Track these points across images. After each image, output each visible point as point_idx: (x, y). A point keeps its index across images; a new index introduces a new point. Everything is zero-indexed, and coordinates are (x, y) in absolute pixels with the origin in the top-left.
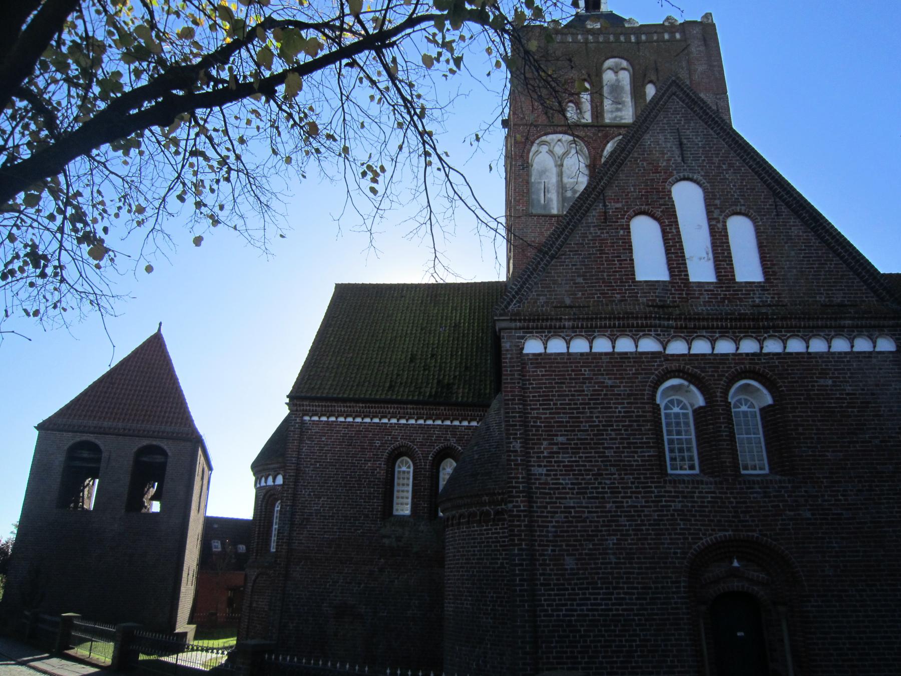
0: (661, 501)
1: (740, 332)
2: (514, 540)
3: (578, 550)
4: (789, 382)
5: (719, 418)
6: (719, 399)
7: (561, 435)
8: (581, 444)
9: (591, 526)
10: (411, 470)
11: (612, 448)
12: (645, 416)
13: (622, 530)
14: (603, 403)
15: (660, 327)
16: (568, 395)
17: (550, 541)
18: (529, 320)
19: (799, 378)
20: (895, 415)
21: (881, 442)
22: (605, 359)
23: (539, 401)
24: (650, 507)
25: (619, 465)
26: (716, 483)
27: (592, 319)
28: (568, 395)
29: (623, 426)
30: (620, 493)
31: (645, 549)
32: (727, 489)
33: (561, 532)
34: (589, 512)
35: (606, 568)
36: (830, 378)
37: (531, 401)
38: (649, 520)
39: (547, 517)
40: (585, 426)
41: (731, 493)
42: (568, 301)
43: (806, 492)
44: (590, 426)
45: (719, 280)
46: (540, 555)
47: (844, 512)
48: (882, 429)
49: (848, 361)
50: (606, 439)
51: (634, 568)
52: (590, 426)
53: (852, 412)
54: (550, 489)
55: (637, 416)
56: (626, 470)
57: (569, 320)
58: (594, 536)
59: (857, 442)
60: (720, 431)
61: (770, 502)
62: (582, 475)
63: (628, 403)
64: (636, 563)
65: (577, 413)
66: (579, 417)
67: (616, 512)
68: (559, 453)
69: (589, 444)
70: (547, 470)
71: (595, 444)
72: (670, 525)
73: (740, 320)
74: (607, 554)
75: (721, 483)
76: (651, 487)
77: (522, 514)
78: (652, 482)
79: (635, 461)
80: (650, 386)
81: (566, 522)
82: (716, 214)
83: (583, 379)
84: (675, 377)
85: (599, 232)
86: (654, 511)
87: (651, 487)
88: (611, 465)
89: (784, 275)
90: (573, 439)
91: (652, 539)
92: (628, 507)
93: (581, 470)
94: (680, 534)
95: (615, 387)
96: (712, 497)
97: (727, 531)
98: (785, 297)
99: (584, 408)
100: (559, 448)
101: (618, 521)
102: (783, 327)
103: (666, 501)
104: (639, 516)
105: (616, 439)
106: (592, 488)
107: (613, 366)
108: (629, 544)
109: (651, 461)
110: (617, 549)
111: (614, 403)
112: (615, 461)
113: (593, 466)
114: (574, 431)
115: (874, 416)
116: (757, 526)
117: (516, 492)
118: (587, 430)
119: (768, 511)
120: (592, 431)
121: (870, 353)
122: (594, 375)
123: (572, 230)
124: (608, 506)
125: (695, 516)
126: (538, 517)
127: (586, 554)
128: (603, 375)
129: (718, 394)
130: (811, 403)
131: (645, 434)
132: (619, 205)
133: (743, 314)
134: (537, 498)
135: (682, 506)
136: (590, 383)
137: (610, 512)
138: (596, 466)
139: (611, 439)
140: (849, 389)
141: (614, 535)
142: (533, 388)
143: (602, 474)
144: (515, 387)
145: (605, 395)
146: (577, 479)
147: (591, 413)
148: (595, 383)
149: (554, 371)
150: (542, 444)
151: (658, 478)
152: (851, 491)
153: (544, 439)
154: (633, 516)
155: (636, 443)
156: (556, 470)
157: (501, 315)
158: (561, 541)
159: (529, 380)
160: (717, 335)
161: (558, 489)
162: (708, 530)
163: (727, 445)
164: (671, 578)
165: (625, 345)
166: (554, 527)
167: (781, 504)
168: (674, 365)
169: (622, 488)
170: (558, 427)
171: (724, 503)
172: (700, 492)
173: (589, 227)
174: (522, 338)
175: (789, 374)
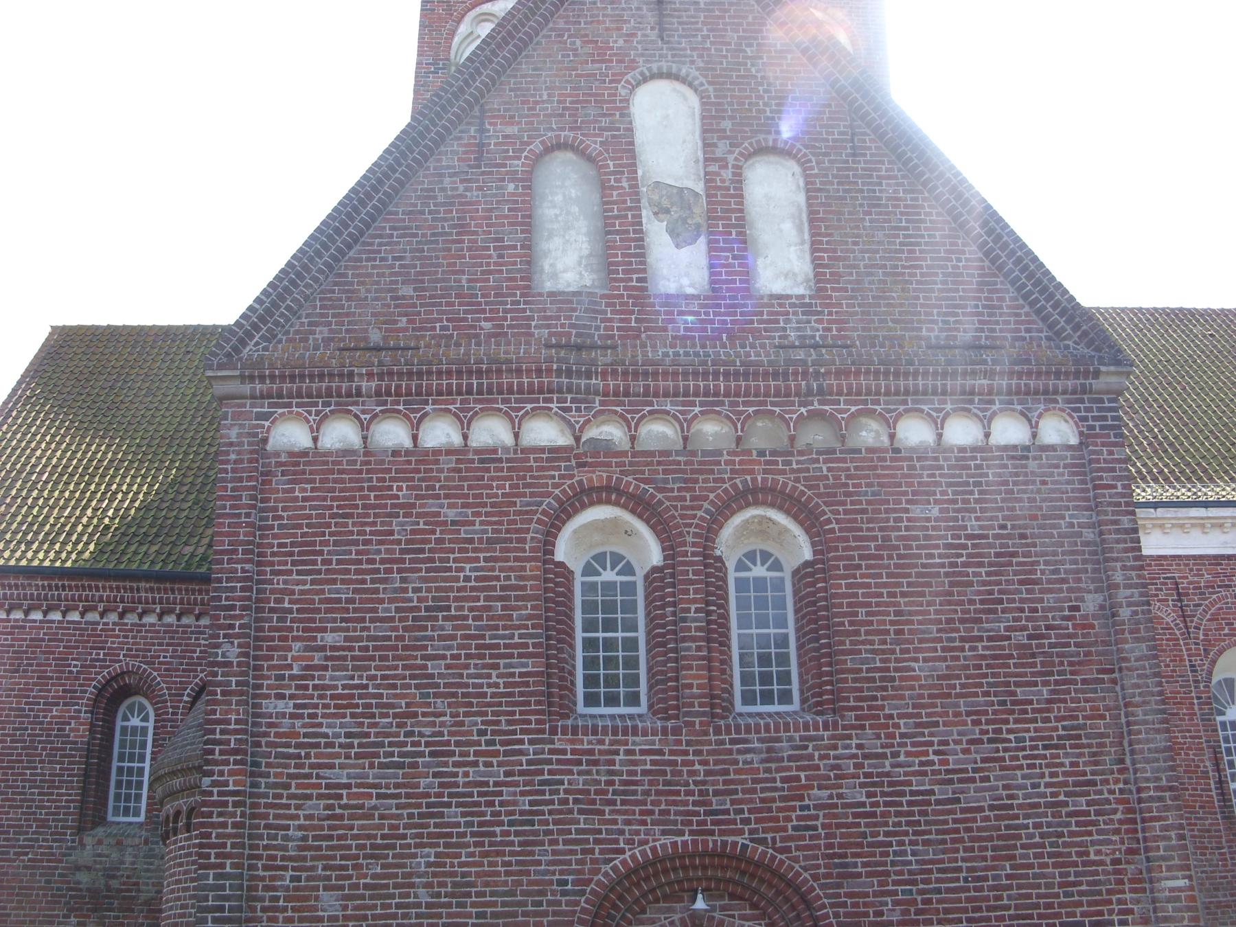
0: (541, 772)
1: (745, 404)
2: (208, 856)
3: (350, 877)
4: (846, 512)
5: (686, 592)
7: (333, 630)
8: (376, 648)
9: (381, 827)
10: (151, 725)
11: (444, 657)
12: (524, 588)
13: (450, 835)
14: (432, 560)
15: (570, 391)
16: (356, 543)
17: (291, 859)
18: (283, 378)
19: (869, 503)
20: (1064, 581)
21: (1030, 637)
22: (448, 463)
23: (291, 554)
24: (516, 784)
25: (454, 695)
26: (665, 731)
27: (420, 374)
28: (356, 543)
29: (471, 609)
30: (453, 754)
31: (498, 874)
32: (688, 743)
33: (315, 838)
34: (379, 796)
36: (936, 502)
37: (273, 554)
39: (288, 807)
40: (386, 609)
41: (696, 753)
42: (375, 337)
43: (859, 746)
44: (398, 610)
45: (714, 290)
46: (267, 888)
47: (936, 788)
48: (1035, 610)
49: (978, 467)
50: (432, 639)
52: (398, 610)
53: (976, 574)
54: (298, 746)
55: (503, 588)
56: (471, 705)
57: (370, 375)
58: (387, 847)
59: (980, 639)
60: (684, 620)
61: (778, 770)
62: (373, 716)
63: (486, 559)
64: (473, 905)
65: (373, 581)
66: (376, 591)
67: (440, 795)
68: (325, 668)
69: (395, 648)
70: (296, 706)
71: (405, 648)
72: (555, 822)
73: (746, 375)
74: (412, 885)
75: (676, 731)
76: (521, 742)
77: (230, 799)
78: (523, 731)
79: (489, 686)
81: (329, 818)
82: (721, 149)
83: (394, 506)
84: (600, 502)
85: (461, 187)
86: (523, 793)
87: (521, 742)
88: (436, 695)
89: (858, 282)
90: (360, 639)
91: (512, 854)
92: (466, 784)
93: (369, 706)
96: (653, 763)
97: (682, 833)
98: (855, 329)
100: (327, 658)
101: (442, 815)
102: (840, 393)
103: (551, 772)
104: (492, 804)
105: (453, 637)
106: (391, 744)
107: (461, 479)
108: (461, 865)
109: (527, 684)
110: (435, 875)
111: (455, 560)
112: (446, 685)
113: (396, 696)
114: (363, 620)
115: (1021, 582)
116: (746, 821)
117: (222, 753)
118: (392, 619)
119: (775, 789)
120: (401, 620)
121: (1026, 448)
122: (418, 497)
123: (402, 184)
124: (423, 782)
125: (612, 803)
126: (267, 806)
127: (366, 886)
128: (438, 497)
129: (690, 539)
130: (890, 557)
131: (519, 627)
132: (512, 130)
133: (752, 364)
134: (268, 765)
136: (406, 515)
137: (428, 795)
138: (404, 696)
139: (441, 638)
140: (972, 526)
141: (432, 845)
142: (281, 527)
143: (415, 715)
144: (239, 525)
145: (439, 541)
146: (361, 724)
147: (403, 580)
148: (419, 515)
149: (333, 490)
150: (290, 649)
151: (538, 722)
152: (956, 742)
153: (295, 639)
154: (478, 804)
155: (497, 646)
156: (316, 706)
157: (221, 367)
158: (313, 858)
159: (275, 509)
160: (697, 409)
161: (317, 745)
163: (699, 649)
165: (491, 431)
166: (300, 828)
167: (802, 774)
168: (598, 477)
169: (458, 744)
170: (327, 611)
171: (680, 773)
172: (628, 752)
173: (442, 175)
174: (266, 416)
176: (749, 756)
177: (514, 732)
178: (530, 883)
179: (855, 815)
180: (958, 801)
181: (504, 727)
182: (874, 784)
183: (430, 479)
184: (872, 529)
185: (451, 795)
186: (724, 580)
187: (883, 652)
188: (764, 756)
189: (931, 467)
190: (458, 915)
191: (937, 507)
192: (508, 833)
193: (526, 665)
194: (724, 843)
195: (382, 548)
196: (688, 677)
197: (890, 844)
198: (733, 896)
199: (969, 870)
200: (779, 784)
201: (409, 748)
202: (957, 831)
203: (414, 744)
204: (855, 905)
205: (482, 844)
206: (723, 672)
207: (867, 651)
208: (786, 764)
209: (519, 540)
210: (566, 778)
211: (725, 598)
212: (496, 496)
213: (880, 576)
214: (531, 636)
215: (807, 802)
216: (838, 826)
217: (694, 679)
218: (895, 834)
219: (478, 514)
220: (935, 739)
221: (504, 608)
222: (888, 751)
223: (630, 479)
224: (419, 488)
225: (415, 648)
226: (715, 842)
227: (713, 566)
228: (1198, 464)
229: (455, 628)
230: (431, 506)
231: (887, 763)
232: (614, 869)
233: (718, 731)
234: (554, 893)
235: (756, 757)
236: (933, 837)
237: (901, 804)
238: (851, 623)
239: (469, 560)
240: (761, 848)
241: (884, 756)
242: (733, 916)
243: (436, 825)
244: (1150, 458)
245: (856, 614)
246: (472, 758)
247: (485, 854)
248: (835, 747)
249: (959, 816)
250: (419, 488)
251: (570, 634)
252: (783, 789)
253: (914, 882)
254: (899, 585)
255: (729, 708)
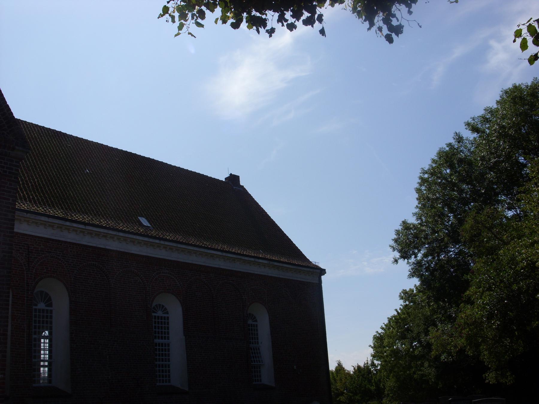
228: (50, 199)
244: (31, 191)
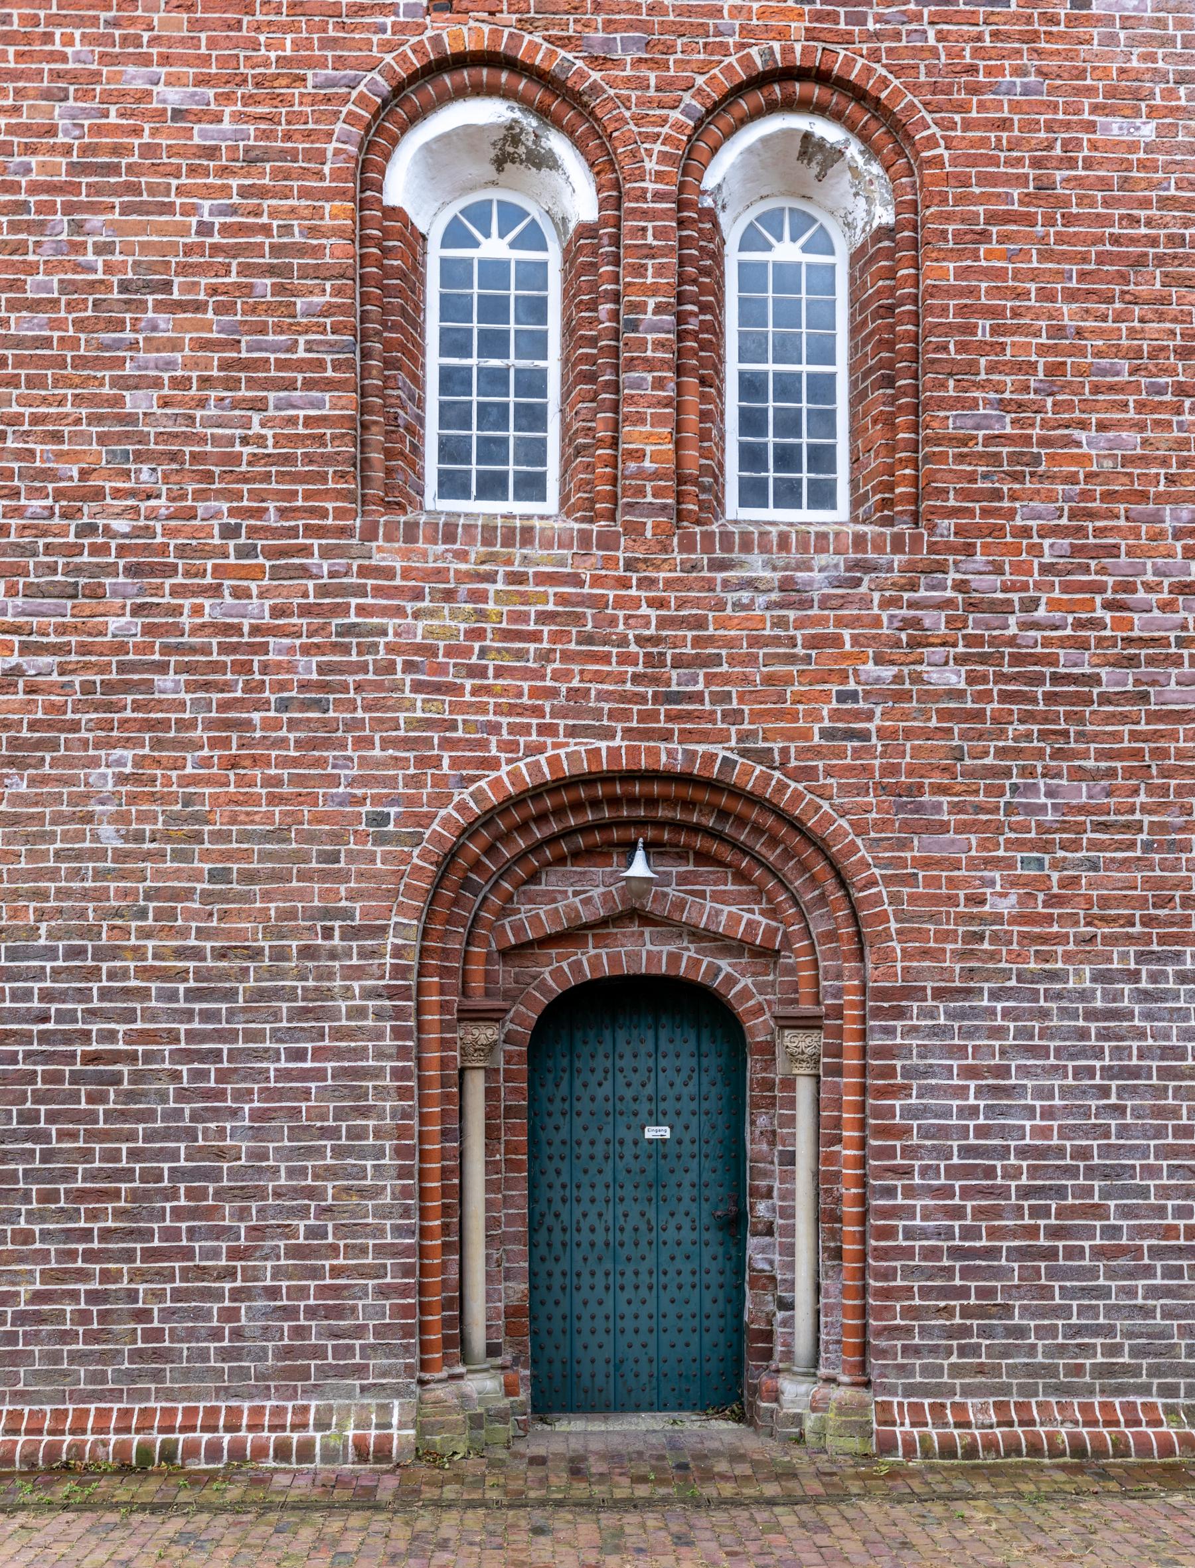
0: (344, 610)
5: (640, 270)
6: (651, 186)
12: (317, 251)
13: (164, 725)
14: (134, 189)
29: (213, 290)
31: (253, 800)
35: (76, 874)
38: (282, 686)
44: (65, 287)
47: (1104, 672)
51: (196, 876)
52: (65, 287)
55: (276, 250)
58: (39, 745)
61: (800, 624)
63: (244, 192)
64: (206, 855)
67: (148, 648)
74: (88, 818)
76: (306, 551)
78: (310, 531)
80: (351, 118)
83: (57, 75)
86: (306, 650)
87: (306, 551)
88: (139, 457)
91: (284, 762)
92: (197, 630)
94: (406, 744)
95: (199, 117)
96: (561, 599)
97: (609, 734)
99: (42, 208)
103: (361, 610)
104: (244, 668)
109: (320, 440)
110: (133, 798)
111: (180, 191)
113: (59, 455)
116: (734, 716)
124: (114, 623)
128: (146, 60)
129: (651, 165)
130: (1050, 221)
135: (429, 633)
137: (121, 648)
141: (127, 743)
145: (149, 150)
148: (109, 97)
151: (339, 513)
152: (1149, 588)
154: (219, 667)
162: (525, 729)
163: (659, 384)
164: (347, 914)
167: (846, 634)
175: (974, 90)
176: (745, 596)
177: (292, 532)
178: (318, 819)
179: (943, 715)
180: (1144, 697)
181: (272, 520)
182: (983, 659)
183: (133, 21)
184: (1019, 161)
185: (167, 649)
186: (717, 257)
187: (1020, 406)
188: (775, 596)
189: (1149, 40)
190: (177, 874)
191: (1153, 124)
192: (275, 725)
193: (319, 405)
194: (690, 756)
195: (33, 160)
196: (633, 435)
197: (1007, 773)
198: (703, 858)
199: (1156, 827)
200: (800, 651)
201: (85, 558)
202: (1137, 754)
203: (96, 550)
204: (931, 882)
205: (225, 743)
206: (704, 435)
207: (988, 403)
208: (815, 611)
209: (309, 155)
210: (391, 623)
211: (718, 290)
212: (266, 63)
213: (1025, 255)
214: (332, 347)
215: (852, 685)
216: (909, 734)
217: (649, 442)
218: (1018, 753)
219: (228, 98)
220: (1110, 580)
221: (279, 289)
222: (1015, 597)
223: (537, 38)
224: (109, 40)
225: (98, 363)
226: (671, 753)
227: (695, 225)
229: (179, 326)
230: (134, 77)
231: (1012, 620)
232: (478, 796)
233: (687, 545)
234: (361, 837)
235: (761, 600)
236: (1090, 764)
237: (1034, 701)
238: (962, 347)
239: (209, 192)
240: (759, 768)
241: (1005, 608)
242: (702, 895)
243: (137, 706)
245: (971, 330)
246: (209, 580)
247: (233, 763)
248: (914, 587)
249: (1143, 727)
250: (109, 40)
251: (416, 353)
252: (807, 659)
253: (1046, 847)
254: (1066, 276)
255: (715, 507)
